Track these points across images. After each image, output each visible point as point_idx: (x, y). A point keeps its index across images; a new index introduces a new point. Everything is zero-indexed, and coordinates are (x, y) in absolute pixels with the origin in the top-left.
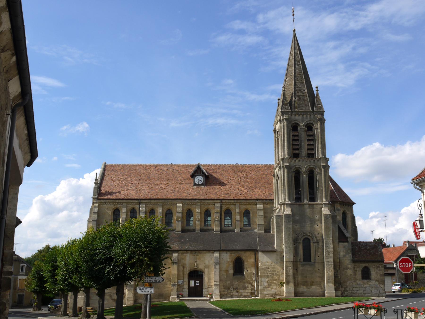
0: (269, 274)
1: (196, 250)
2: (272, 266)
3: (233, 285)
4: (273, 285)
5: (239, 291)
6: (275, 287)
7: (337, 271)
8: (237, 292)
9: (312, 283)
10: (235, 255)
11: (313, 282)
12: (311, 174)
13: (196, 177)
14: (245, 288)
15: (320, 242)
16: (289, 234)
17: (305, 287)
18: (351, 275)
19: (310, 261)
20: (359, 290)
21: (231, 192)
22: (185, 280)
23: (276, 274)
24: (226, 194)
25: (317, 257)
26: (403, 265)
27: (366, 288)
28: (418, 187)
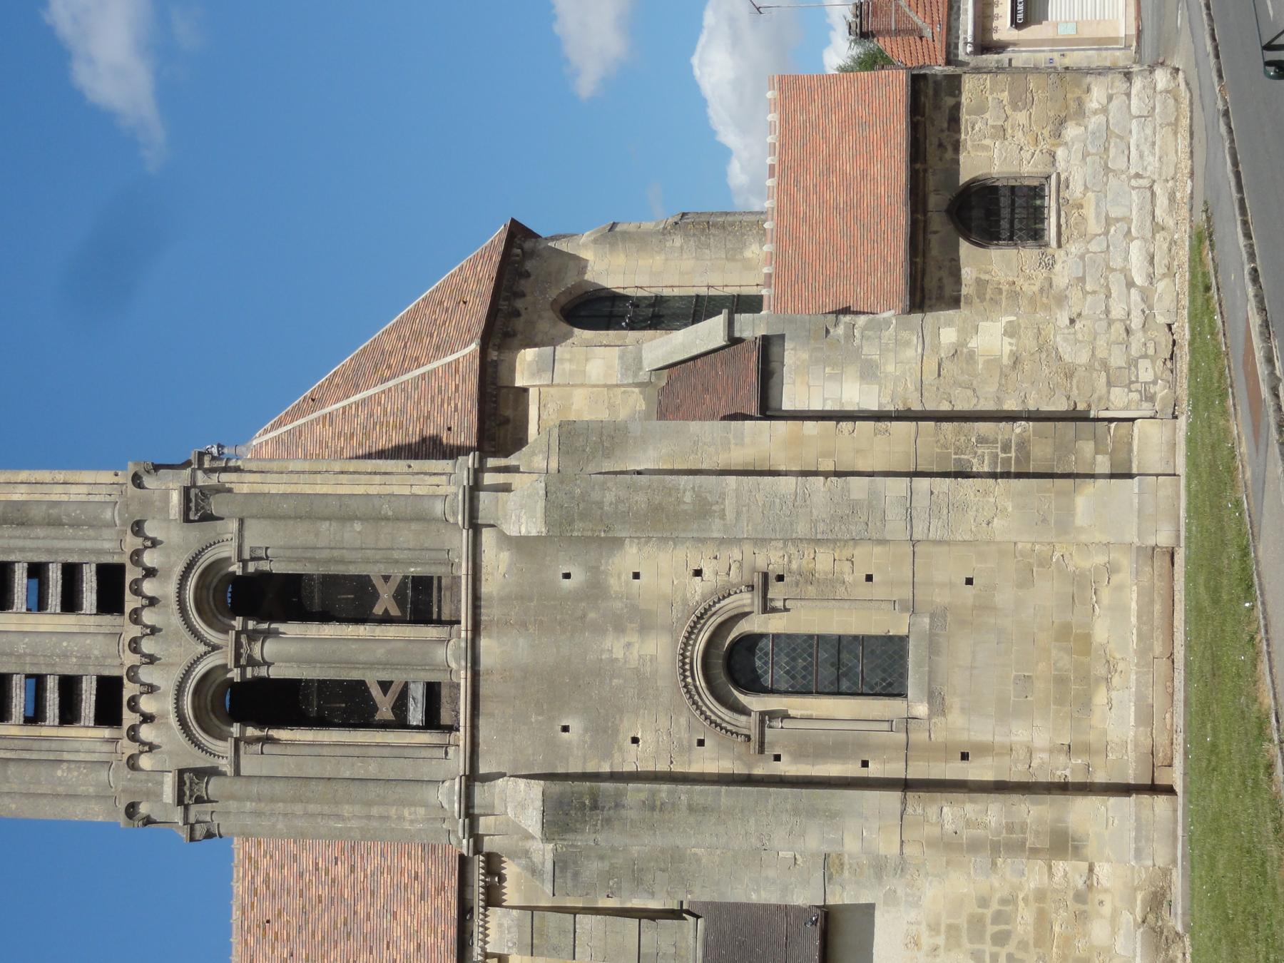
2: (941, 940)
6: (1099, 931)
7: (982, 440)
9: (1075, 639)
11: (1064, 633)
15: (761, 563)
16: (691, 809)
17: (1100, 697)
18: (1011, 331)
19: (903, 640)
23: (998, 917)
27: (1109, 221)
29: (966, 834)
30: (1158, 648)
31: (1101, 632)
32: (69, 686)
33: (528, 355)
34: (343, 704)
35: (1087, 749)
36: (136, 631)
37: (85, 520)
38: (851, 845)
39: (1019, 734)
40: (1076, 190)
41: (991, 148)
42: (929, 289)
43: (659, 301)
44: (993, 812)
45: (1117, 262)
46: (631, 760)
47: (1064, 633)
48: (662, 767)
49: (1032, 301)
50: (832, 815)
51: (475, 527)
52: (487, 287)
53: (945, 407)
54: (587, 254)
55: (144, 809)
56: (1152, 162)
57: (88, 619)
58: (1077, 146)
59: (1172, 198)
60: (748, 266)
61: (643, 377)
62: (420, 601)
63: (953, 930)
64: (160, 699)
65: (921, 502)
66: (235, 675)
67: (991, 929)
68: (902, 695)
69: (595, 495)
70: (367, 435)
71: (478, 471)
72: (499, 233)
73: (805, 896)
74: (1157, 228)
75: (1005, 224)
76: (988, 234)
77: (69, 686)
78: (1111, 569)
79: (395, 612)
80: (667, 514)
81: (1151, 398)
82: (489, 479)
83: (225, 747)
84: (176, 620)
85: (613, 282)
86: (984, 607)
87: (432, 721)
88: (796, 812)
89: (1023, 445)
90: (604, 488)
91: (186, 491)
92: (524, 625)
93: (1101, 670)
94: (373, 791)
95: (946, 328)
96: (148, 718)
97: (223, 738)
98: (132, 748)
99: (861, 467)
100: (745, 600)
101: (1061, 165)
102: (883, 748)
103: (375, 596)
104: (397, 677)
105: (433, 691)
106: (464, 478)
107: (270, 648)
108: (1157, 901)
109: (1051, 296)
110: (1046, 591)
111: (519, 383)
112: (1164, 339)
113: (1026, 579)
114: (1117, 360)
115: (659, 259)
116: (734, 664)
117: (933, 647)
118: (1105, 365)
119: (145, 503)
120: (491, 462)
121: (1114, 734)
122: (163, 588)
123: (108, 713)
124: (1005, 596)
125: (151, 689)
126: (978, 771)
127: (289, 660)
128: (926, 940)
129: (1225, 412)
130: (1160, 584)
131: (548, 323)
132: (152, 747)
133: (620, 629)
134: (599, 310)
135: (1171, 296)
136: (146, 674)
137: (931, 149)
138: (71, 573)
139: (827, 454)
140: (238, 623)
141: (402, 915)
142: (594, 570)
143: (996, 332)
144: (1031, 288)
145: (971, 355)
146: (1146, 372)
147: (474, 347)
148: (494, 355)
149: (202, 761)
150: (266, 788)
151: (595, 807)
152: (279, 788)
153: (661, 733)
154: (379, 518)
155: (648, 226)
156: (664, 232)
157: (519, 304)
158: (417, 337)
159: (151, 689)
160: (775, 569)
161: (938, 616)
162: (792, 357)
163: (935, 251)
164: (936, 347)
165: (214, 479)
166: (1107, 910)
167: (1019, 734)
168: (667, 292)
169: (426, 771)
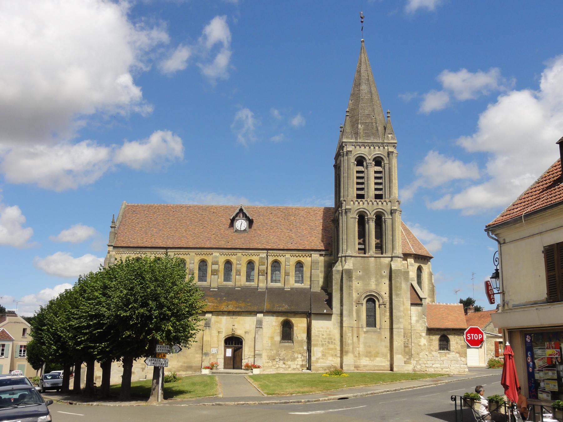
1: (234, 312)
3: (279, 355)
4: (328, 355)
5: (286, 362)
6: (330, 358)
7: (408, 340)
8: (284, 364)
9: (377, 355)
10: (281, 319)
11: (378, 353)
12: (379, 219)
14: (294, 359)
17: (367, 359)
19: (375, 327)
21: (280, 240)
23: (332, 342)
24: (274, 243)
25: (383, 323)
26: (471, 336)
27: (443, 361)
28: (493, 236)
31: (378, 359)
32: (362, 189)
35: (359, 356)
39: (361, 346)
40: (448, 356)
41: (455, 341)
42: (431, 331)
43: (421, 283)
45: (436, 362)
47: (378, 353)
62: (380, 247)
63: (330, 335)
65: (400, 330)
67: (330, 341)
72: (431, 255)
74: (442, 369)
76: (440, 340)
77: (362, 189)
84: (375, 208)
86: (381, 340)
92: (376, 265)
93: (372, 359)
96: (359, 203)
100: (381, 301)
102: (358, 323)
109: (431, 351)
111: (408, 260)
112: (424, 370)
114: (420, 362)
117: (375, 332)
118: (420, 360)
121: (362, 361)
122: (380, 206)
125: (363, 204)
130: (386, 369)
133: (376, 281)
135: (431, 371)
141: (316, 239)
142: (385, 277)
144: (432, 348)
158: (413, 241)
161: (380, 333)
162: (419, 308)
163: (438, 332)
167: (361, 346)
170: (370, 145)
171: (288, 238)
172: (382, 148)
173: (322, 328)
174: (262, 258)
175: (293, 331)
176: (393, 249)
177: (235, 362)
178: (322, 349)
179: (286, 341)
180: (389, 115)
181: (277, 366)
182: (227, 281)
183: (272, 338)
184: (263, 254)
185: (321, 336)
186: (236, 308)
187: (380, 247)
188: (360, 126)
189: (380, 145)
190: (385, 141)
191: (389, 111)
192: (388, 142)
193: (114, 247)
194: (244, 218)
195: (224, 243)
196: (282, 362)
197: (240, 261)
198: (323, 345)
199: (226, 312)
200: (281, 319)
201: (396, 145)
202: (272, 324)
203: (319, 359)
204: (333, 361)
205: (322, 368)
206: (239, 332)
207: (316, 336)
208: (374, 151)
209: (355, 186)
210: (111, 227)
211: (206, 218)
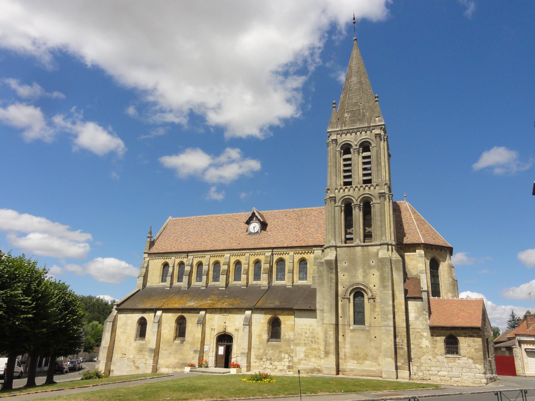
0: (306, 342)
1: (225, 309)
2: (311, 331)
4: (310, 356)
6: (313, 360)
7: (403, 340)
8: (271, 364)
9: (365, 357)
10: (269, 316)
12: (367, 206)
13: (251, 225)
14: (280, 360)
15: (377, 298)
16: (331, 286)
17: (355, 362)
18: (427, 347)
20: (441, 371)
22: (212, 345)
23: (315, 341)
29: (328, 335)
30: (364, 373)
31: (367, 362)
32: (350, 177)
33: (422, 252)
34: (349, 224)
35: (345, 359)
36: (359, 186)
37: (379, 176)
38: (325, 315)
39: (348, 346)
40: (458, 361)
42: (435, 330)
43: (438, 277)
44: (332, 340)
45: (443, 369)
46: (340, 275)
48: (339, 280)
49: (434, 351)
50: (331, 311)
51: (380, 245)
52: (437, 244)
53: (411, 333)
54: (446, 262)
55: (329, 191)
56: (465, 378)
57: (362, 178)
58: (467, 362)
59: (458, 381)
60: (446, 294)
61: (419, 274)
62: (368, 236)
63: (313, 333)
64: (348, 192)
65: (389, 328)
66: (353, 204)
67: (313, 340)
68: (354, 324)
69: (386, 267)
70: (407, 223)
71: (392, 245)
72: (449, 245)
73: (318, 306)
74: (451, 378)
75: (450, 346)
77: (350, 177)
78: (379, 365)
79: (367, 231)
80: (387, 281)
81: (415, 375)
82: (390, 247)
83: (340, 204)
84: (361, 193)
85: (441, 268)
86: (371, 340)
87: (347, 239)
88: (331, 305)
89: (402, 348)
90: (388, 268)
91: (384, 193)
92: (363, 255)
93: (360, 362)
94: (333, 230)
95: (427, 333)
97: (342, 203)
98: (339, 189)
99: (396, 317)
101: (463, 358)
102: (344, 320)
103: (369, 228)
104: (354, 232)
105: (351, 239)
106: (390, 242)
107: (357, 210)
108: (319, 371)
109: (435, 355)
110: (374, 352)
112: (427, 378)
113: (376, 348)
114: (422, 368)
115: (447, 276)
116: (358, 293)
117: (363, 330)
118: (421, 365)
119: (382, 186)
120: (394, 247)
122: (367, 191)
123: (346, 184)
124: (373, 344)
126: (341, 338)
127: (355, 213)
128: (311, 328)
129: (390, 389)
130: (376, 374)
131: (430, 255)
132: (339, 192)
133: (363, 272)
134: (434, 266)
135: (436, 380)
136: (352, 189)
137: (464, 331)
138: (370, 174)
139: (398, 310)
140: (362, 204)
141: (321, 235)
143: (426, 345)
144: (436, 351)
145: (421, 339)
146: (420, 374)
147: (423, 242)
148: (422, 246)
149: (337, 200)
150: (333, 212)
151: (331, 269)
152: (333, 214)
153: (345, 280)
154: (381, 227)
155: (454, 274)
156: (452, 277)
157: (434, 250)
159: (349, 191)
160: (376, 300)
161: (368, 331)
162: (419, 303)
163: (442, 332)
164: (423, 332)
165: (387, 198)
166: (317, 361)
167: (348, 346)
168: (440, 278)
169: (337, 239)
170: (355, 130)
171: (295, 236)
172: (368, 132)
173: (305, 325)
174: (267, 256)
175: (280, 329)
176: (383, 234)
177: (226, 361)
178: (304, 349)
179: (275, 340)
180: (377, 99)
181: (264, 366)
182: (238, 281)
183: (260, 336)
184: (268, 253)
185: (304, 334)
186: (230, 305)
187: (368, 236)
188: (346, 115)
189: (366, 129)
190: (372, 125)
191: (376, 95)
192: (375, 125)
193: (149, 254)
194: (257, 221)
195: (235, 244)
196: (269, 362)
197: (247, 260)
198: (305, 344)
199: (218, 309)
200: (269, 316)
201: (383, 127)
202: (260, 321)
203: (301, 360)
204: (316, 363)
205: (304, 370)
206: (230, 330)
207: (299, 334)
208: (360, 136)
209: (343, 174)
210: (148, 237)
211: (229, 225)
